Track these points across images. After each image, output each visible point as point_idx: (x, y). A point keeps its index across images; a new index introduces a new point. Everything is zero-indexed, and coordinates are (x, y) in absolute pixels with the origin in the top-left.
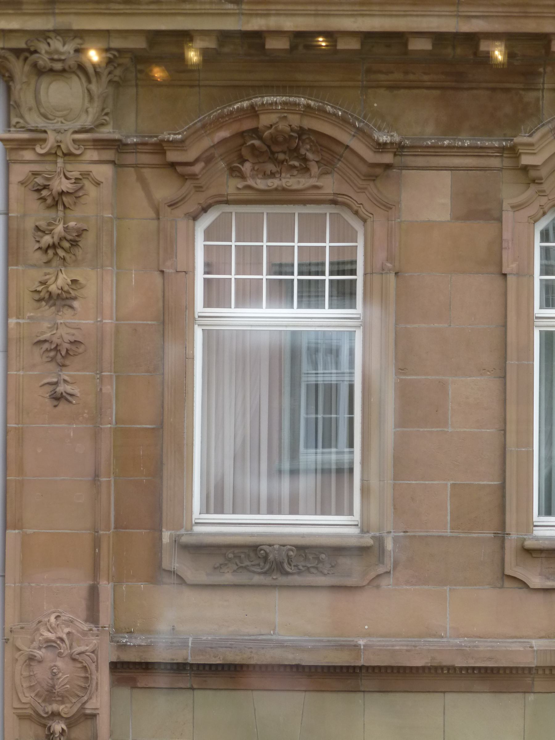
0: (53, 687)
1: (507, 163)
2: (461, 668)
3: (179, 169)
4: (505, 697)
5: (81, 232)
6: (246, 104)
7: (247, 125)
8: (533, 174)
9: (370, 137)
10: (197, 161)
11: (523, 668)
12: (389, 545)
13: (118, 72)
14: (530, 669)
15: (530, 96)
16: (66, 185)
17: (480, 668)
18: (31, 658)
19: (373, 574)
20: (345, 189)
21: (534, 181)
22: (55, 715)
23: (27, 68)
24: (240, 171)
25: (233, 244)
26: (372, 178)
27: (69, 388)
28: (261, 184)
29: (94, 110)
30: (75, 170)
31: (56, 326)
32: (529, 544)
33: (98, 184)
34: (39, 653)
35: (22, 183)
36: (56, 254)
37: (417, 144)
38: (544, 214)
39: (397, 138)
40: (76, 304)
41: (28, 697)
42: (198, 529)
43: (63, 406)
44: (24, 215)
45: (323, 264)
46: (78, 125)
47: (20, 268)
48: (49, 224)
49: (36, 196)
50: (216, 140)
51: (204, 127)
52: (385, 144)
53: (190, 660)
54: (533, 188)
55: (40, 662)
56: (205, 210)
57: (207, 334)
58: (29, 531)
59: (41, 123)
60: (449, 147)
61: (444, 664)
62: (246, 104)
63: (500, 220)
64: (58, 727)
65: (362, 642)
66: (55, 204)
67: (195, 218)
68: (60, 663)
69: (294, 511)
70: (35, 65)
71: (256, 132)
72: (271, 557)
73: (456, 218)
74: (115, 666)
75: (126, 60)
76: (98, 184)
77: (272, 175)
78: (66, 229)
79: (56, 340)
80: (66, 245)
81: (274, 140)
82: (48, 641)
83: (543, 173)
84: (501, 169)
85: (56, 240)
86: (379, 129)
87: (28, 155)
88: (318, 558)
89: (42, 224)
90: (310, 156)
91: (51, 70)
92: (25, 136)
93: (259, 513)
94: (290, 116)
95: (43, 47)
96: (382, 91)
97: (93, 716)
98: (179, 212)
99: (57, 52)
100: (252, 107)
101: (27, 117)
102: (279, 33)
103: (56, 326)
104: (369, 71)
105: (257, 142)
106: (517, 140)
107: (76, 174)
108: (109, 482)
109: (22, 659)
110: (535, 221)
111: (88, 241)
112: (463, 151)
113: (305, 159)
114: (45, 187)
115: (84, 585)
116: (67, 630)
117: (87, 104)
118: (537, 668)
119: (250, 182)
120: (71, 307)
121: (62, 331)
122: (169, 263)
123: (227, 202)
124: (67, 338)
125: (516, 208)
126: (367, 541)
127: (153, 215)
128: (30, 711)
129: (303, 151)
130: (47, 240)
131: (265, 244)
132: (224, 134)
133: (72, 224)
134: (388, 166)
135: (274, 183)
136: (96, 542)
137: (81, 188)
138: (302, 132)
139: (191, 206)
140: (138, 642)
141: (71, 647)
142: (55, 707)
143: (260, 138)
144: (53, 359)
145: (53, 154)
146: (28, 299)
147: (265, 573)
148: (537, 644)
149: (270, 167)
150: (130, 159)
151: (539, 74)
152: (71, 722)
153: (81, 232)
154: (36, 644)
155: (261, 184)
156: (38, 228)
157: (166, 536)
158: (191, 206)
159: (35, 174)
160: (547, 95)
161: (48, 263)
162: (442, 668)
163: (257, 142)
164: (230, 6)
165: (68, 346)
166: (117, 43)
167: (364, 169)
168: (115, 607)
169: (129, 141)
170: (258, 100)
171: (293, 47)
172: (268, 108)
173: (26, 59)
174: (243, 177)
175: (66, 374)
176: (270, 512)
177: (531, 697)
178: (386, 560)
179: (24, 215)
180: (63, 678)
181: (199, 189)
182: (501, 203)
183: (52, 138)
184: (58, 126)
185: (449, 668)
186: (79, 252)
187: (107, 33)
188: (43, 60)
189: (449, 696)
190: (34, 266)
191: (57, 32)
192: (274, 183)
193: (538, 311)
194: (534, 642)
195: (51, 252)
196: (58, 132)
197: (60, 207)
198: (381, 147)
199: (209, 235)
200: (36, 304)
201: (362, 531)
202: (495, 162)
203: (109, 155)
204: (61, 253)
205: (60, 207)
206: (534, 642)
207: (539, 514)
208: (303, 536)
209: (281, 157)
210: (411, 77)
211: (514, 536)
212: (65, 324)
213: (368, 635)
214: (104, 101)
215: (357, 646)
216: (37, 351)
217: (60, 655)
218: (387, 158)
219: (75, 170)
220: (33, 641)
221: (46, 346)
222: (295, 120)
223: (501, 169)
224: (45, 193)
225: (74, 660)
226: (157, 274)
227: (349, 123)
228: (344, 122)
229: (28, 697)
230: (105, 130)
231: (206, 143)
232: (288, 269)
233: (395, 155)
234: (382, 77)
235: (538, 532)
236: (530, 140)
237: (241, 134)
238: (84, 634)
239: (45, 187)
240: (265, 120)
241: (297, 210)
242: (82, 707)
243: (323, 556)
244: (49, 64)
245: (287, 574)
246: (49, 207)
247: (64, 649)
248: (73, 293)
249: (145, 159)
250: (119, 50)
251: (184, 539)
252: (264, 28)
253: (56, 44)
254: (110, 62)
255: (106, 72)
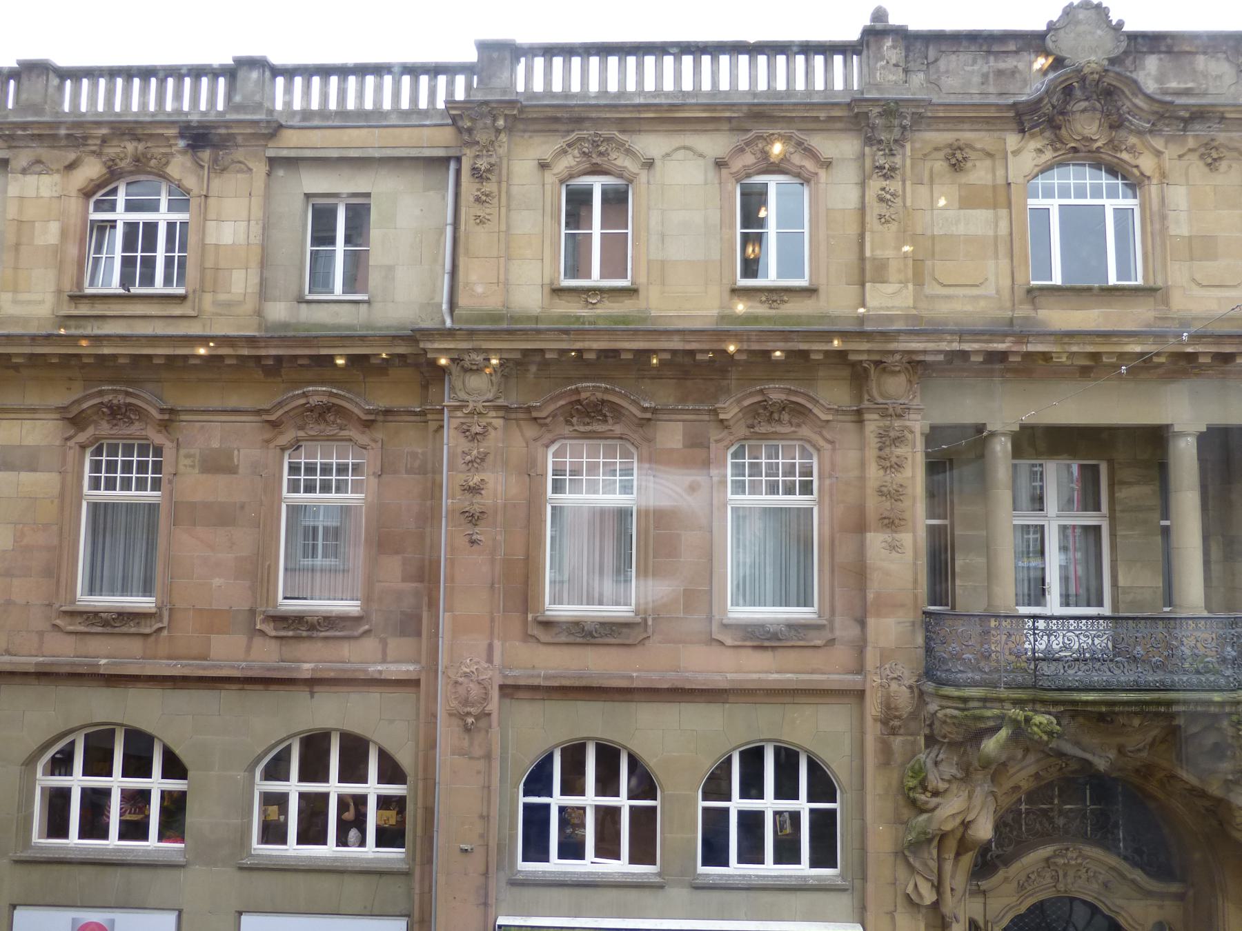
0: (468, 698)
1: (712, 418)
2: (689, 689)
3: (539, 421)
4: (712, 705)
5: (486, 454)
6: (573, 387)
7: (574, 398)
8: (726, 423)
9: (639, 404)
10: (548, 416)
11: (722, 690)
12: (650, 622)
13: (507, 370)
14: (726, 690)
15: (725, 383)
16: (478, 430)
17: (698, 689)
18: (456, 682)
19: (641, 638)
20: (626, 431)
21: (726, 428)
22: (468, 714)
23: (458, 368)
24: (571, 422)
25: (568, 460)
26: (641, 426)
27: (479, 537)
28: (582, 429)
29: (494, 390)
30: (483, 422)
31: (472, 504)
32: (725, 621)
33: (496, 429)
34: (460, 680)
35: (456, 428)
36: (473, 466)
37: (665, 407)
38: (732, 445)
39: (653, 405)
40: (483, 492)
41: (454, 704)
42: (547, 613)
43: (475, 546)
44: (456, 446)
45: (566, 471)
46: (485, 398)
47: (454, 473)
48: (470, 450)
49: (463, 435)
50: (558, 406)
51: (551, 399)
52: (647, 408)
53: (542, 684)
54: (726, 431)
55: (461, 684)
56: (553, 442)
57: (554, 508)
58: (457, 613)
59: (466, 397)
60: (681, 409)
61: (679, 687)
62: (573, 387)
63: (709, 448)
64: (470, 720)
65: (635, 674)
66: (473, 440)
67: (547, 446)
68: (471, 685)
69: (601, 603)
70: (463, 367)
71: (579, 402)
72: (586, 628)
73: (685, 446)
74: (502, 687)
75: (511, 364)
76: (496, 429)
77: (588, 424)
78: (478, 452)
79: (472, 512)
80: (478, 461)
81: (588, 404)
82: (465, 673)
83: (731, 423)
84: (709, 421)
85: (473, 458)
86: (644, 400)
87: (459, 414)
88: (611, 629)
89: (466, 450)
90: (608, 414)
91: (471, 369)
92: (458, 404)
93: (582, 604)
94: (597, 393)
95: (467, 358)
96: (647, 381)
97: (489, 715)
98: (539, 443)
99: (474, 360)
100: (577, 388)
101: (459, 394)
102: (267, 357)
103: (472, 504)
104: (638, 370)
105: (579, 407)
106: (716, 406)
107: (484, 424)
108: (499, 588)
109: (452, 682)
110: (728, 449)
111: (490, 458)
112: (688, 411)
113: (605, 416)
114: (468, 431)
115: (486, 642)
116: (476, 667)
117: (490, 387)
118: (730, 689)
119: (576, 428)
120: (481, 494)
121: (476, 506)
122: (533, 470)
123: (565, 438)
124: (478, 510)
125: (717, 441)
126: (638, 620)
127: (525, 445)
128: (455, 712)
129: (604, 412)
130: (468, 458)
131: (585, 460)
132: (562, 402)
133: (482, 450)
134: (649, 420)
135: (588, 428)
136: (492, 620)
137: (487, 431)
138: (603, 402)
139: (545, 441)
140: (514, 674)
141: (478, 676)
142: (469, 709)
143: (581, 405)
144: (471, 521)
145: (472, 413)
146: (458, 489)
147: (583, 637)
148: (729, 676)
149: (587, 420)
150: (513, 416)
151: (728, 371)
152: (477, 718)
153: (486, 454)
154: (459, 675)
155: (582, 429)
156: (463, 452)
157: (530, 617)
158: (545, 441)
159: (463, 424)
160: (733, 382)
161: (469, 470)
162: (678, 689)
163: (579, 407)
164: (564, 336)
165: (478, 514)
166: (505, 356)
167: (637, 421)
168: (502, 655)
169: (513, 406)
170: (579, 385)
171: (598, 358)
172: (586, 389)
173: (458, 364)
174: (573, 425)
175: (477, 530)
176: (599, 605)
177: (727, 706)
178: (648, 630)
179: (456, 446)
180: (473, 693)
181: (549, 431)
182: (709, 439)
183: (471, 405)
184: (474, 399)
185: (681, 689)
186: (485, 465)
187: (500, 350)
188: (467, 364)
189: (682, 704)
190: (461, 472)
191: (474, 350)
192: (588, 428)
193: (730, 496)
194: (728, 675)
195: (470, 465)
196: (475, 401)
197: (476, 441)
198: (645, 410)
199: (555, 456)
200: (462, 492)
201: (636, 615)
202: (706, 417)
203: (501, 413)
204: (476, 465)
205: (476, 441)
206: (728, 675)
207: (732, 605)
208: (604, 617)
209: (593, 414)
210: (661, 373)
211: (717, 617)
212: (477, 503)
213: (638, 670)
214: (499, 386)
215: (632, 677)
216: (462, 517)
217: (472, 680)
218: (648, 415)
219: (483, 422)
220: (457, 673)
221: (467, 514)
222: (599, 395)
223: (709, 421)
224: (467, 433)
225: (479, 683)
226: (527, 476)
227: (627, 396)
228: (625, 396)
229: (454, 704)
230: (502, 400)
231: (552, 407)
232: (563, 473)
233: (653, 413)
234: (646, 373)
235: (731, 615)
236: (723, 406)
237: (571, 403)
238: (485, 669)
239: (468, 431)
240: (583, 395)
241: (602, 442)
242: (483, 710)
243: (614, 628)
244: (470, 366)
245: (595, 637)
246: (470, 441)
247: (474, 677)
248: (482, 486)
249: (521, 416)
250: (507, 359)
251: (540, 619)
252: (582, 348)
253: (474, 356)
254: (501, 365)
255: (500, 370)
